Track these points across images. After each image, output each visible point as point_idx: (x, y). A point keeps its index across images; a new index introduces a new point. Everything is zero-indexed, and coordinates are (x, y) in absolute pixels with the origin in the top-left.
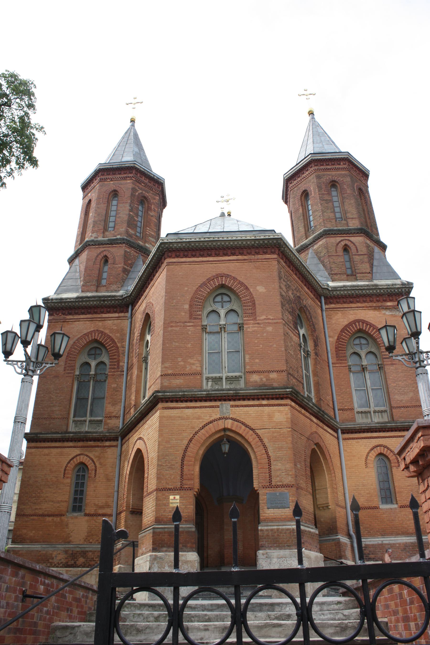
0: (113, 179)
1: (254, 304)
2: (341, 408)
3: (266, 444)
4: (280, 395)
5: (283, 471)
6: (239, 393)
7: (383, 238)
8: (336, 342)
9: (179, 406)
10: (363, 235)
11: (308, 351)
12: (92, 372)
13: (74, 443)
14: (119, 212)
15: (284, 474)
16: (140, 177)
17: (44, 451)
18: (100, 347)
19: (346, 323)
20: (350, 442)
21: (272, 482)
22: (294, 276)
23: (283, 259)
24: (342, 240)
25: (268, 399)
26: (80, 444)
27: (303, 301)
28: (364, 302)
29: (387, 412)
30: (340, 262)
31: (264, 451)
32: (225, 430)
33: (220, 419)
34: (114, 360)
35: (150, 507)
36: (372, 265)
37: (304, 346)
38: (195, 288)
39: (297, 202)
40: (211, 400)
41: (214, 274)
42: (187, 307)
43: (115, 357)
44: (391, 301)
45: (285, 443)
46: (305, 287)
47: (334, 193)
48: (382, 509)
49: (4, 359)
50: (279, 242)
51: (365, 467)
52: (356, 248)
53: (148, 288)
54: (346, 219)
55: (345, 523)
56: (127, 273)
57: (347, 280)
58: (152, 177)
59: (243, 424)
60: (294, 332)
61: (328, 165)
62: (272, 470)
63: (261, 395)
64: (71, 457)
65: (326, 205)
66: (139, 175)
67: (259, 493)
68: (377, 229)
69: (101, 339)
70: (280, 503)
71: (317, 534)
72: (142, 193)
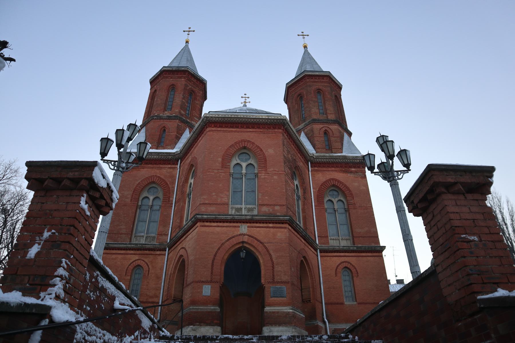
0: (172, 78)
1: (266, 160)
2: (320, 235)
3: (271, 253)
4: (281, 221)
5: (283, 272)
6: (254, 218)
7: (349, 128)
8: (318, 192)
9: (212, 225)
10: (337, 124)
11: (299, 196)
13: (134, 251)
14: (175, 99)
15: (283, 274)
16: (191, 77)
17: (112, 256)
18: (157, 187)
19: (324, 180)
20: (326, 259)
21: (275, 280)
22: (292, 145)
23: (285, 133)
24: (323, 127)
25: (273, 223)
27: (297, 163)
28: (337, 167)
29: (350, 240)
30: (321, 141)
31: (270, 258)
32: (243, 242)
33: (240, 235)
34: (166, 196)
35: (188, 295)
36: (343, 144)
37: (297, 192)
38: (226, 148)
39: (294, 102)
40: (234, 222)
41: (240, 140)
43: (167, 194)
44: (354, 167)
45: (283, 253)
46: (299, 154)
47: (319, 97)
48: (346, 305)
49: (101, 158)
50: (284, 121)
51: (335, 276)
52: (333, 132)
53: (193, 148)
54: (326, 114)
55: (321, 313)
56: (178, 139)
57: (326, 153)
58: (198, 78)
59: (255, 239)
60: (292, 182)
61: (316, 79)
62: (275, 271)
63: (269, 220)
64: (131, 261)
65: (314, 104)
66: (190, 76)
67: (265, 287)
68: (346, 122)
69: (158, 181)
70: (280, 294)
71: (304, 317)
72: (191, 88)
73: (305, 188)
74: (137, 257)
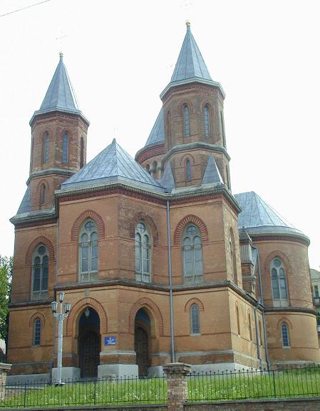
12: (41, 263)
26: (36, 307)
42: (70, 233)
73: (157, 234)
74: (35, 311)
